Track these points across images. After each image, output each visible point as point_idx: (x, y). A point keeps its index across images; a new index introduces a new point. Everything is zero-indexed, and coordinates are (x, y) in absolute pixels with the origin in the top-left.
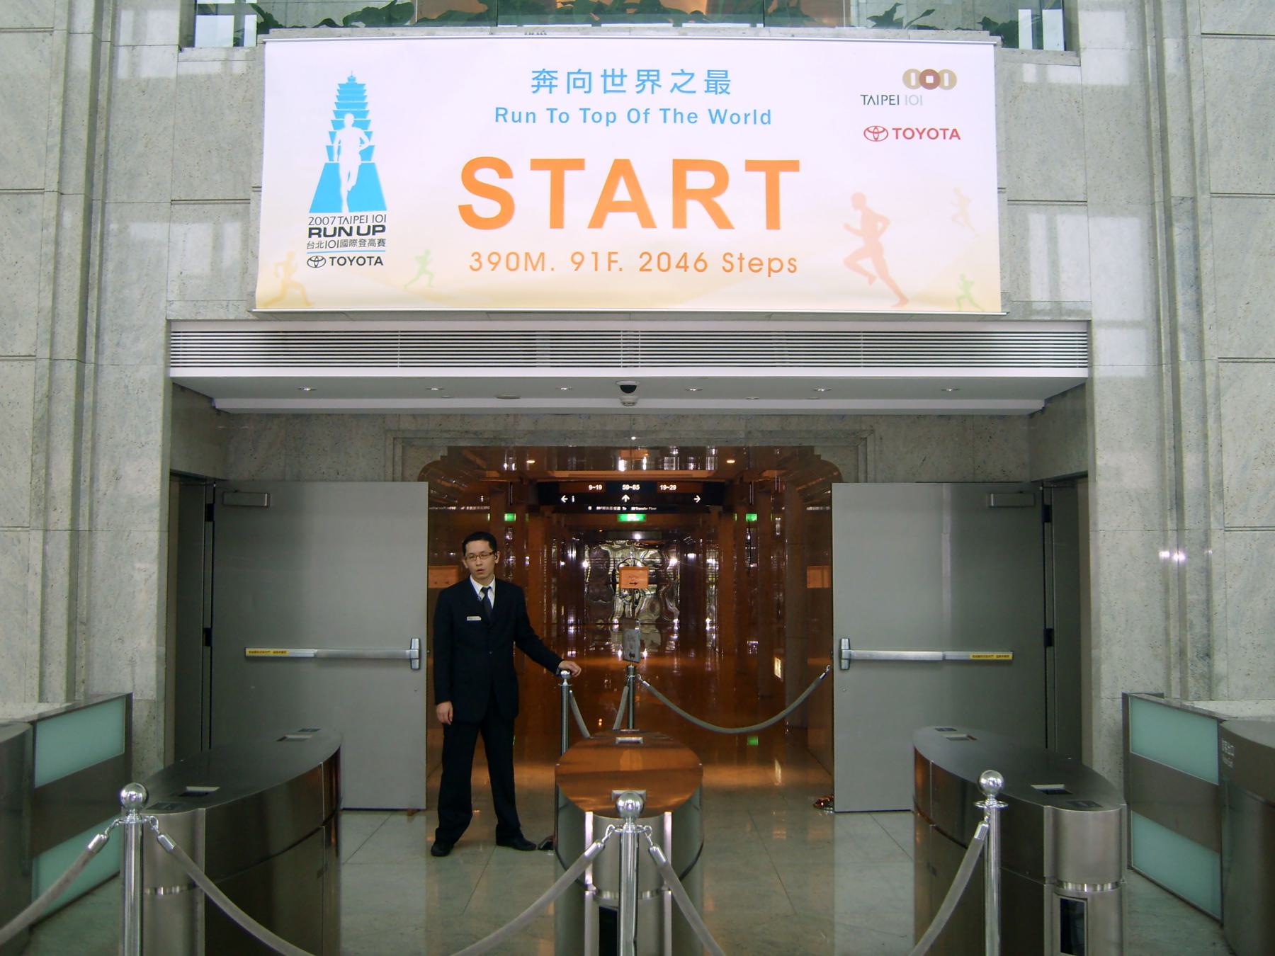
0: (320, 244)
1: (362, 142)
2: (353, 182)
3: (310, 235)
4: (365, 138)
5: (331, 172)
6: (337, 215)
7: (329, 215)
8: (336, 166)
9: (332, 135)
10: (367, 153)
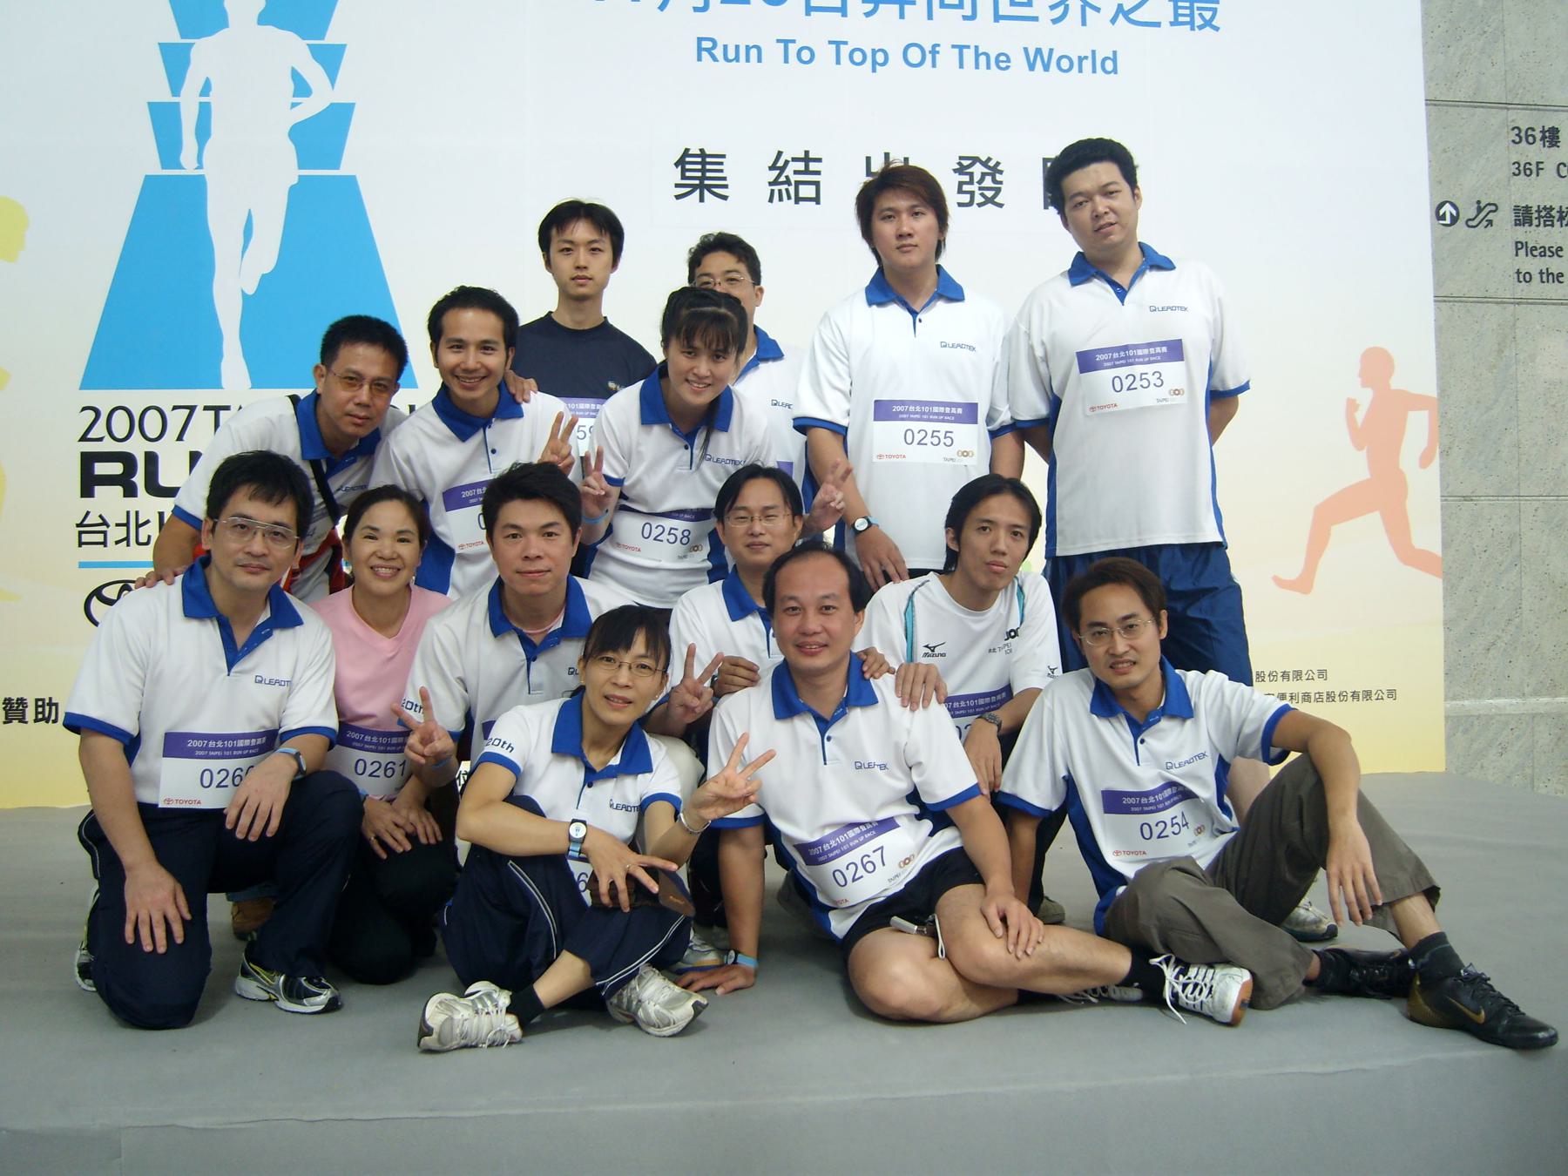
0: (132, 524)
1: (302, 88)
2: (265, 254)
3: (89, 483)
4: (314, 73)
5: (169, 221)
6: (201, 397)
7: (166, 398)
8: (195, 188)
9: (176, 61)
10: (321, 137)
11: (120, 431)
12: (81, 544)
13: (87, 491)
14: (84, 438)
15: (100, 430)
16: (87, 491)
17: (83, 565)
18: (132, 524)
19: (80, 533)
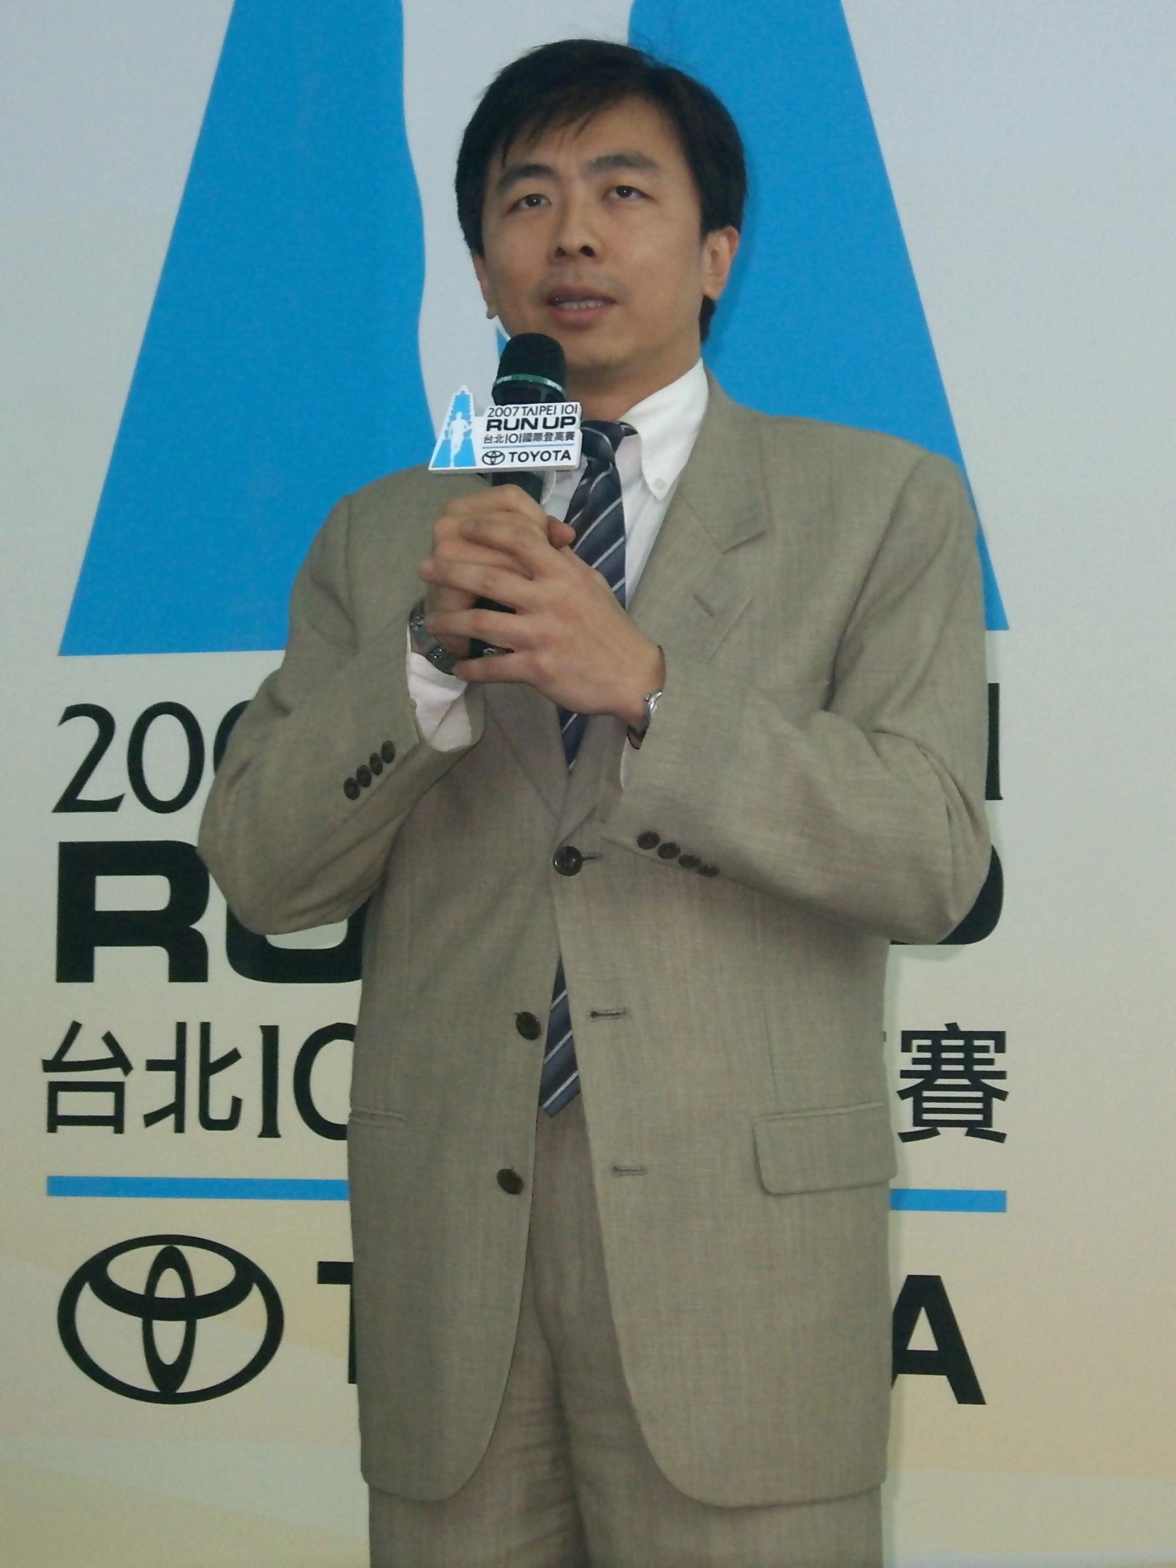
0: (194, 1059)
3: (82, 937)
11: (165, 777)
12: (55, 1121)
13: (74, 965)
14: (70, 802)
15: (110, 778)
16: (74, 965)
17: (60, 1186)
18: (194, 1059)
19: (55, 1088)
